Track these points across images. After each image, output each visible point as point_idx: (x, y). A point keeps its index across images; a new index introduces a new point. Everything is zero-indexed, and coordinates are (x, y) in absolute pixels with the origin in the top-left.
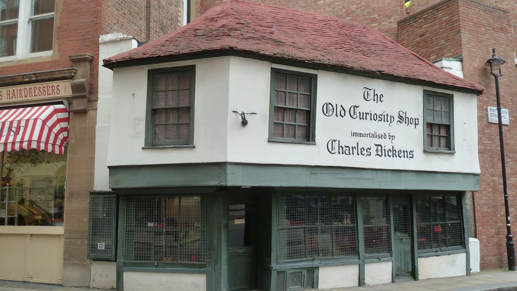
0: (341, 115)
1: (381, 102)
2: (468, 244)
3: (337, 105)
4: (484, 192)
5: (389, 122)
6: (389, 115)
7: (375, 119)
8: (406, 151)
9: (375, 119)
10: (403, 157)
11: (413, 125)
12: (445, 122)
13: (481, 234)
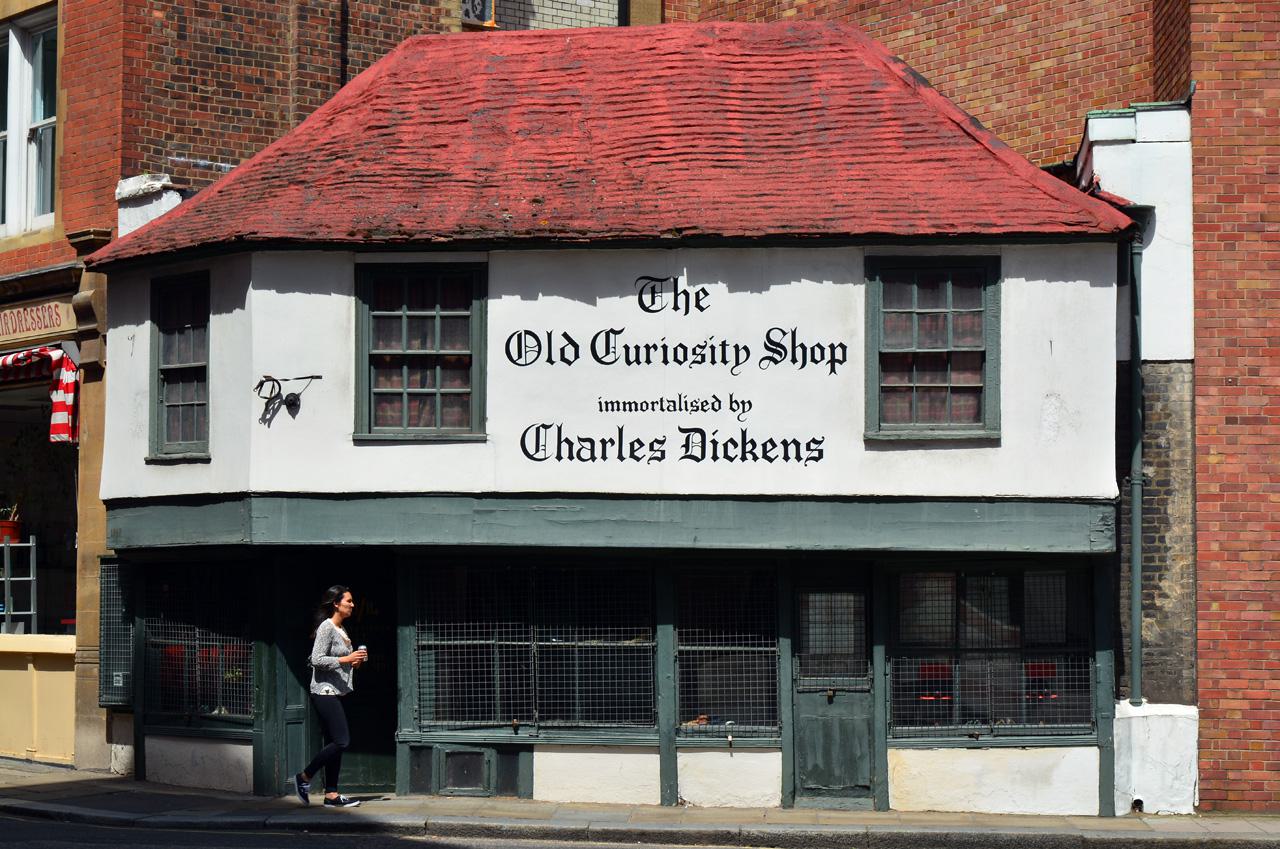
0: (563, 359)
1: (702, 309)
3: (549, 335)
5: (732, 363)
7: (680, 357)
8: (795, 442)
9: (680, 357)
11: (825, 367)
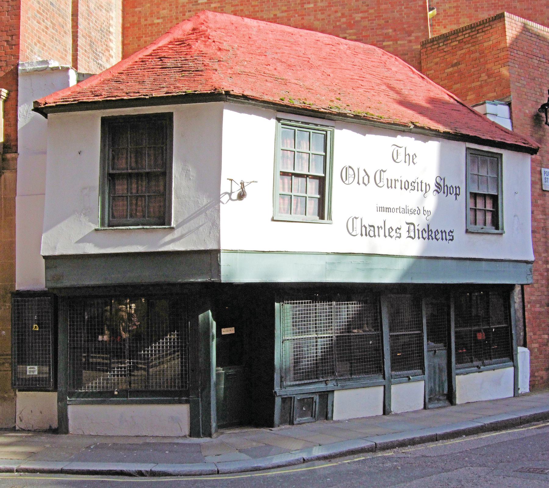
0: (364, 183)
1: (414, 164)
2: (516, 354)
3: (358, 169)
4: (536, 285)
5: (424, 192)
6: (424, 182)
7: (407, 187)
9: (407, 187)
10: (440, 239)
11: (453, 196)
12: (494, 193)
13: (532, 342)
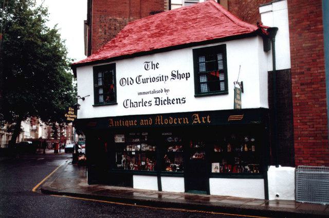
11: (185, 79)
